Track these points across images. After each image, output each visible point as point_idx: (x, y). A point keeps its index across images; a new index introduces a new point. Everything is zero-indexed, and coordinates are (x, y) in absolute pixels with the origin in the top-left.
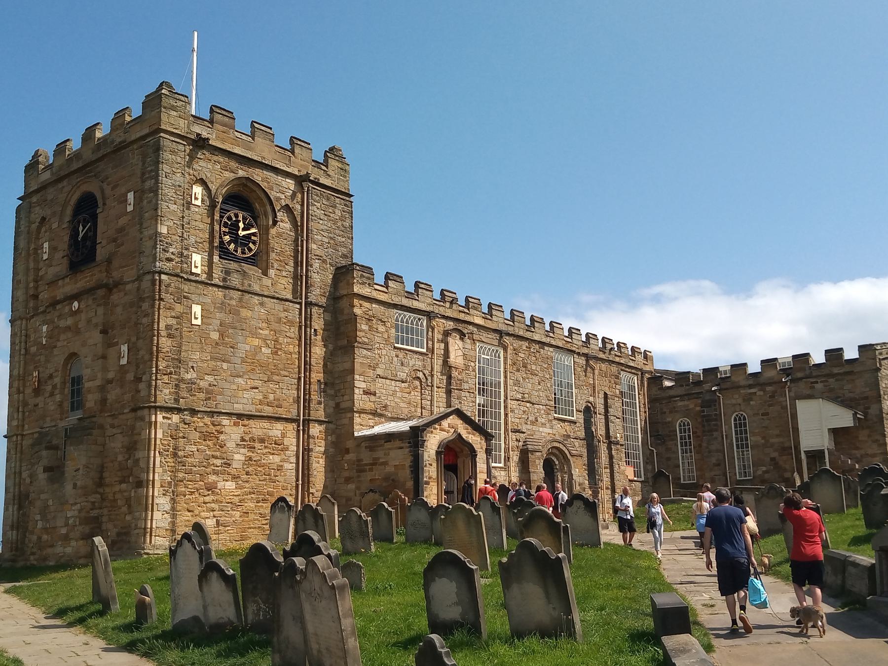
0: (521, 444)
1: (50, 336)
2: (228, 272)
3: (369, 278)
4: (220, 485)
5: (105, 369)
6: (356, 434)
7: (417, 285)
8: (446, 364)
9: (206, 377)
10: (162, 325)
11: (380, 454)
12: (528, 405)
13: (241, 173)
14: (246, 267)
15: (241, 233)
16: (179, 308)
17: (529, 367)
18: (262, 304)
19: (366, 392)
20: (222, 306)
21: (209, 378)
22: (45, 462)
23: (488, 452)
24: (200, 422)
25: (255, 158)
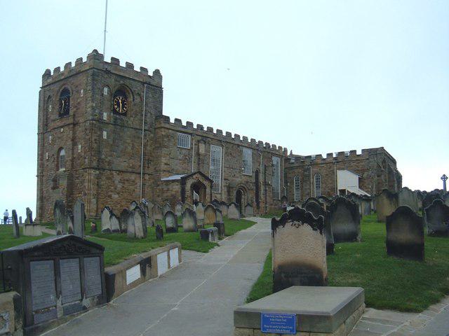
1: (52, 140)
2: (116, 119)
5: (73, 154)
7: (187, 123)
8: (198, 154)
11: (170, 187)
13: (122, 82)
20: (114, 132)
21: (109, 158)
22: (52, 186)
23: (211, 187)
25: (127, 76)
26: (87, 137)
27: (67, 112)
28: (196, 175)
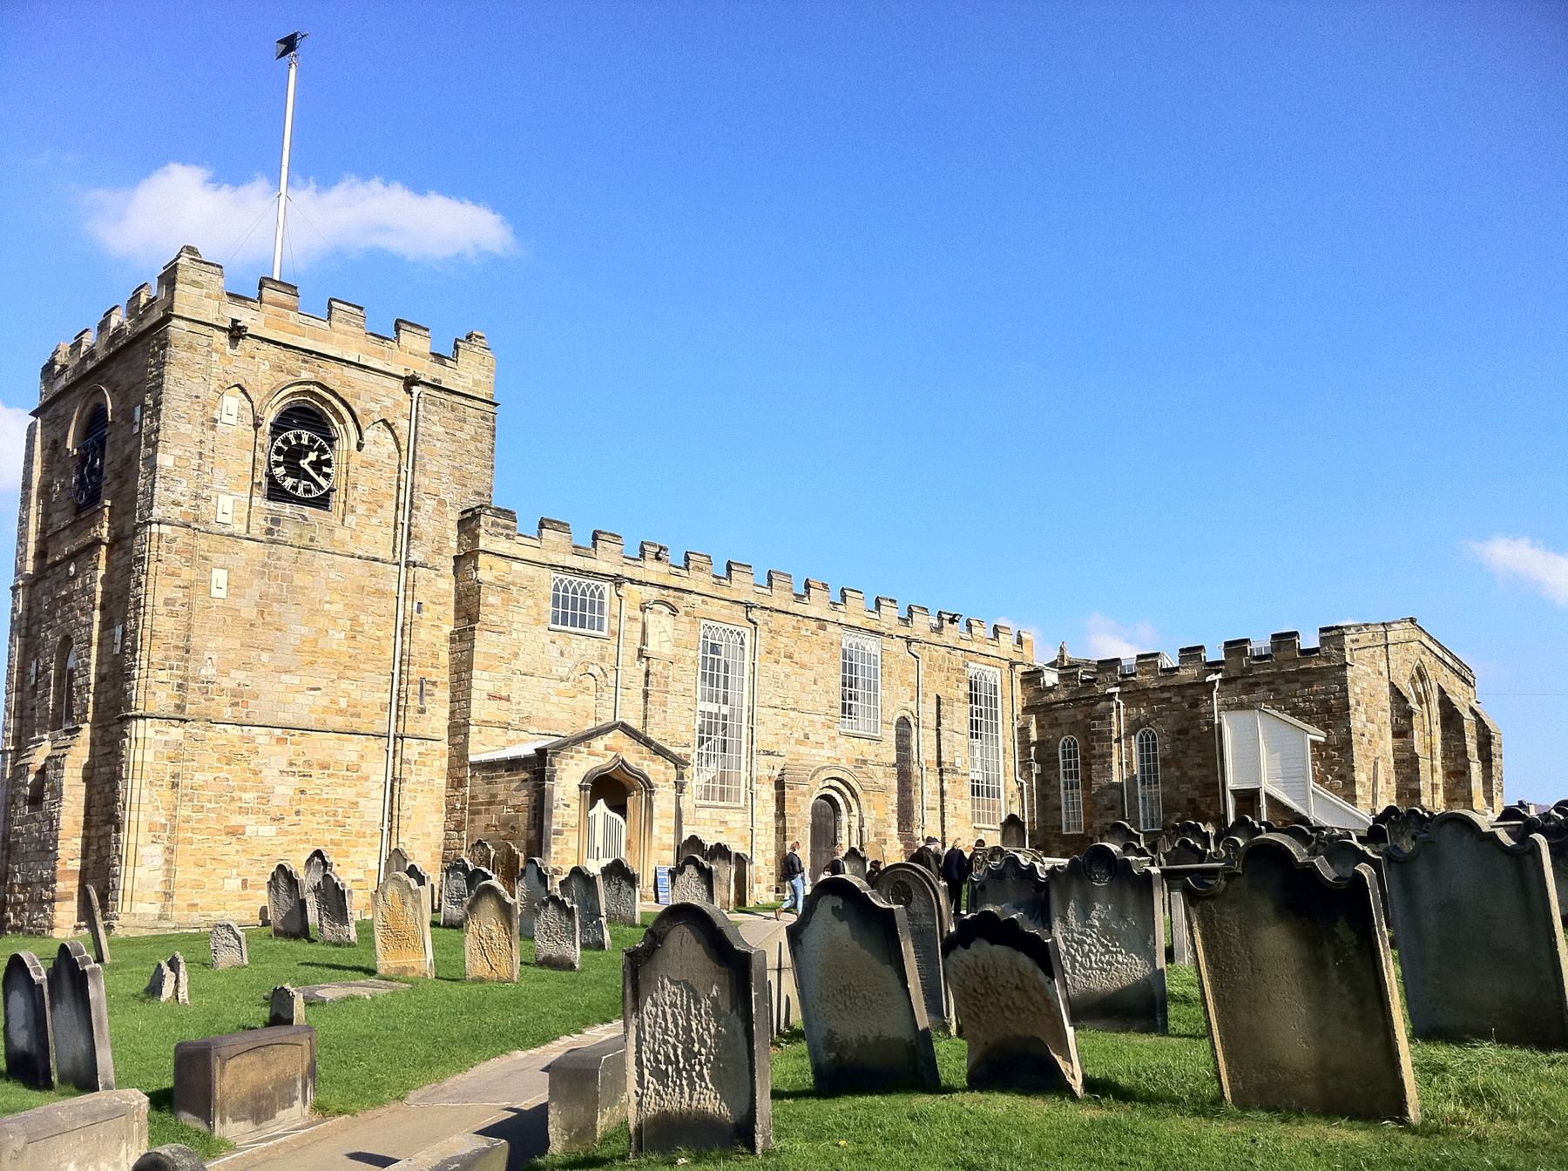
0: (776, 773)
3: (507, 527)
4: (249, 831)
6: (472, 758)
9: (233, 674)
10: (160, 601)
12: (792, 714)
13: (305, 375)
14: (308, 511)
15: (304, 463)
16: (187, 574)
17: (796, 657)
18: (331, 566)
19: (492, 697)
20: (264, 570)
21: (239, 676)
23: (680, 786)
24: (218, 735)
28: (608, 739)
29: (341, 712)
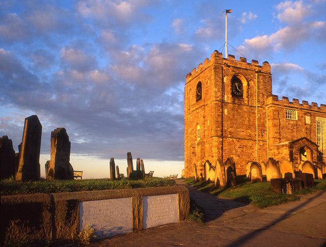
11: (280, 151)
21: (231, 129)
26: (213, 114)
27: (200, 98)
29: (248, 136)
